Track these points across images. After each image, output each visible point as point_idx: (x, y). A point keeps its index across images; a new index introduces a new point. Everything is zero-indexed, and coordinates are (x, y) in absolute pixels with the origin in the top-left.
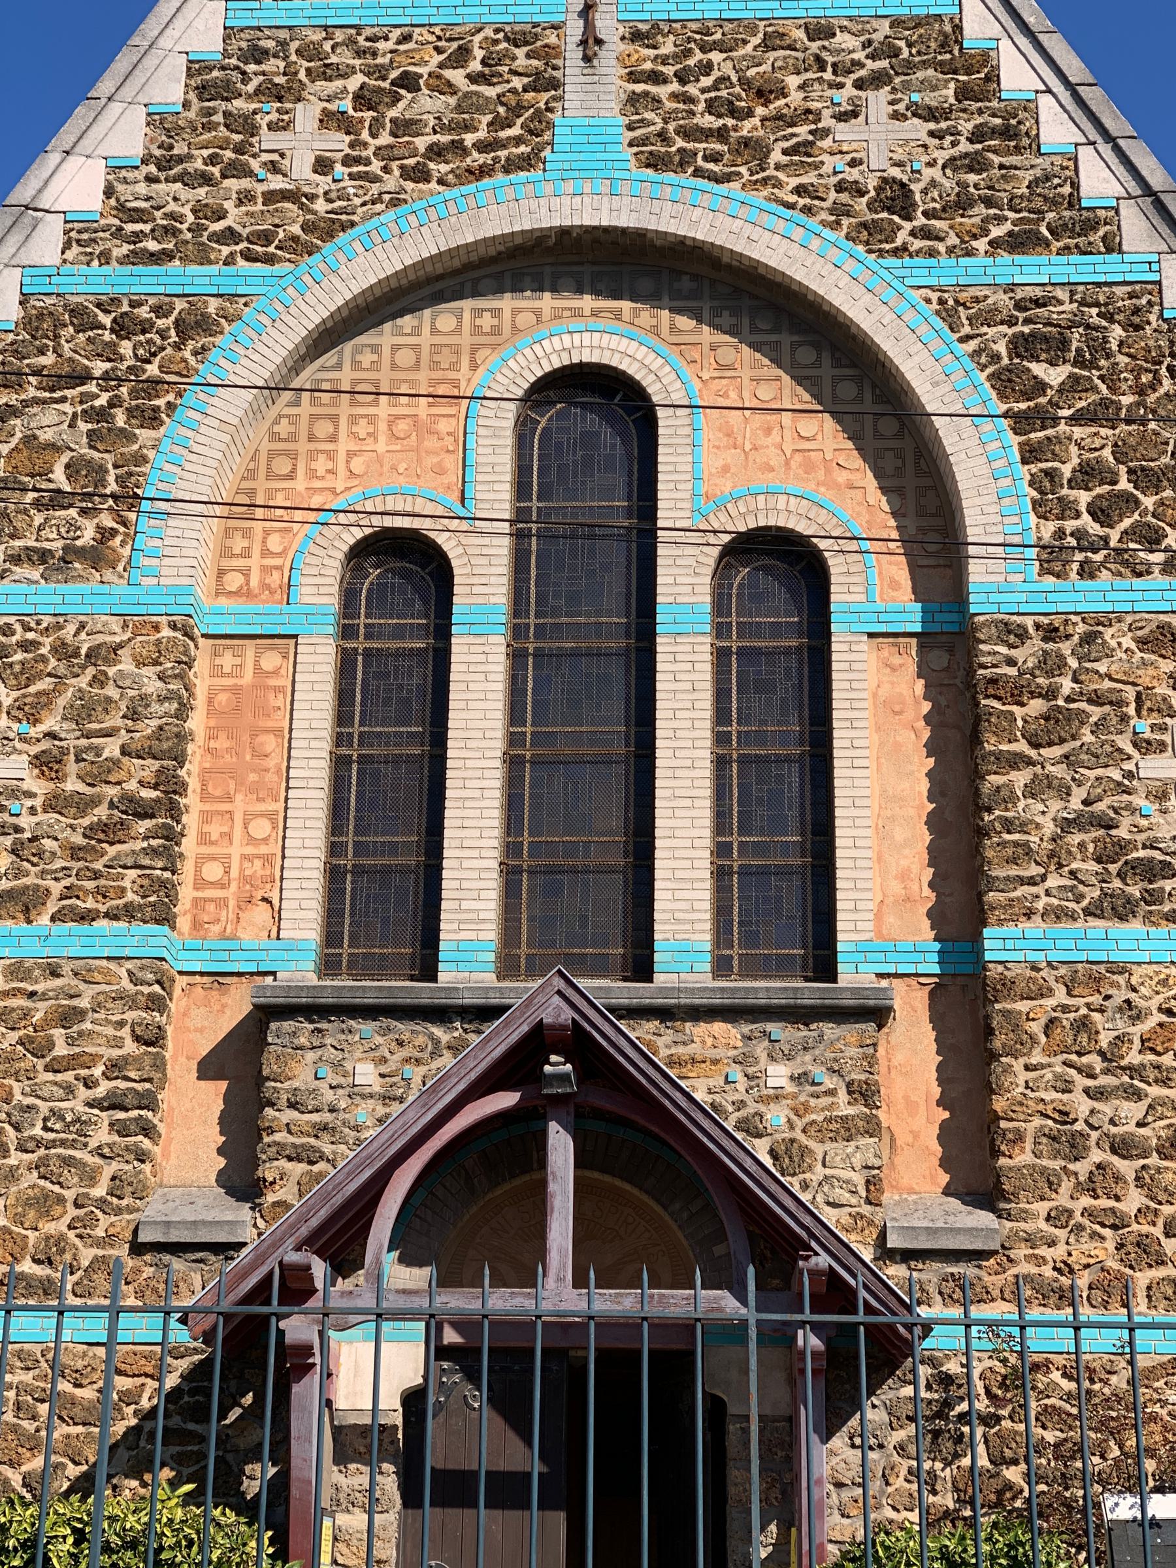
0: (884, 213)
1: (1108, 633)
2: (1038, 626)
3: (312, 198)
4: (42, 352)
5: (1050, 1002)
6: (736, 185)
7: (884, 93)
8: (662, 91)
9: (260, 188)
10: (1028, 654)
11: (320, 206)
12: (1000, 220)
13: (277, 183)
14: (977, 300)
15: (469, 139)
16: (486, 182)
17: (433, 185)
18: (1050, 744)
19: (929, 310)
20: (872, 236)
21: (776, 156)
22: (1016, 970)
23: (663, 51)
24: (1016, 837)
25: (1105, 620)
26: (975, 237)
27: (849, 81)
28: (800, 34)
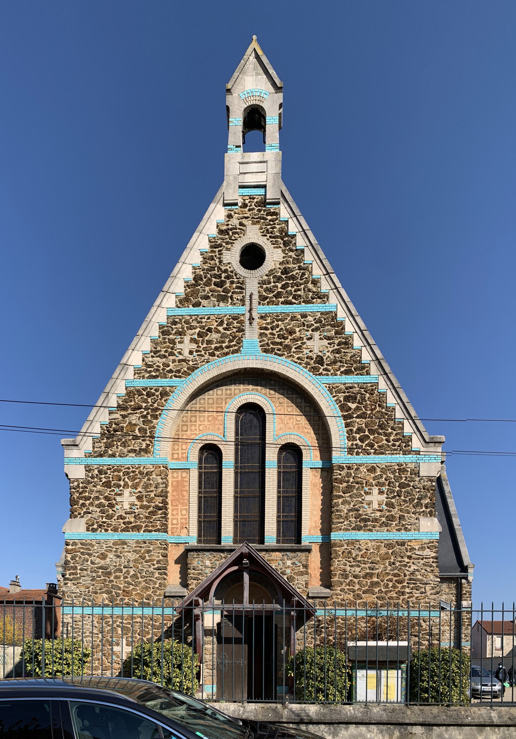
1: (361, 468)
25: (360, 465)
27: (310, 329)
28: (299, 317)
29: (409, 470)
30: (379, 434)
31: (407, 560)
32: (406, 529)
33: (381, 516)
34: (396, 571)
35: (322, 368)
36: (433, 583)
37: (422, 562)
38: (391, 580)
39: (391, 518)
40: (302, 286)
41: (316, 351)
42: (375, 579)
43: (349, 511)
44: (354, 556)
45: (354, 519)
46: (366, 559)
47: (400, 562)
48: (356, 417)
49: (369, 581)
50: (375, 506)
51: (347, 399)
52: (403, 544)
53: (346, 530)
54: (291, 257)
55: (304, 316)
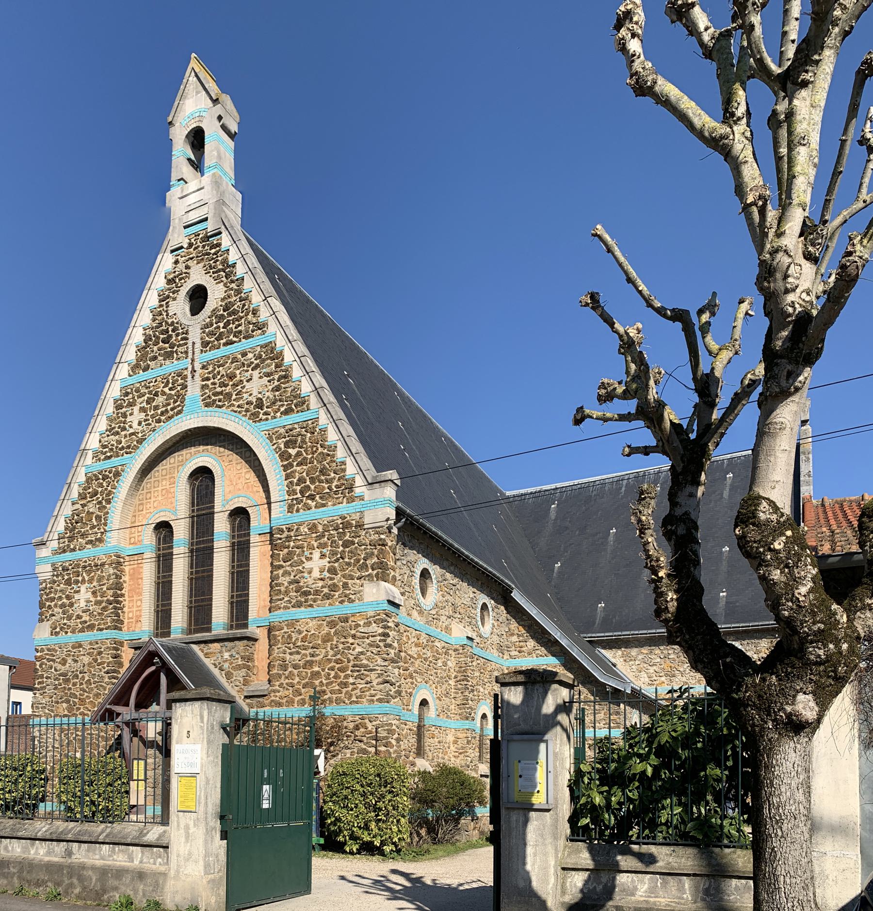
0: (256, 411)
1: (302, 527)
7: (258, 371)
8: (209, 383)
15: (169, 408)
20: (254, 417)
21: (234, 397)
25: (300, 524)
27: (250, 369)
28: (240, 356)
29: (354, 522)
30: (321, 481)
31: (351, 640)
32: (351, 601)
33: (322, 587)
34: (339, 656)
35: (262, 412)
36: (380, 668)
37: (368, 641)
38: (332, 669)
39: (333, 588)
40: (243, 320)
41: (255, 393)
42: (316, 669)
43: (290, 583)
44: (294, 639)
45: (295, 594)
46: (306, 644)
47: (343, 643)
48: (298, 465)
49: (309, 671)
50: (316, 574)
51: (287, 445)
52: (346, 620)
53: (286, 608)
54: (232, 289)
55: (244, 354)
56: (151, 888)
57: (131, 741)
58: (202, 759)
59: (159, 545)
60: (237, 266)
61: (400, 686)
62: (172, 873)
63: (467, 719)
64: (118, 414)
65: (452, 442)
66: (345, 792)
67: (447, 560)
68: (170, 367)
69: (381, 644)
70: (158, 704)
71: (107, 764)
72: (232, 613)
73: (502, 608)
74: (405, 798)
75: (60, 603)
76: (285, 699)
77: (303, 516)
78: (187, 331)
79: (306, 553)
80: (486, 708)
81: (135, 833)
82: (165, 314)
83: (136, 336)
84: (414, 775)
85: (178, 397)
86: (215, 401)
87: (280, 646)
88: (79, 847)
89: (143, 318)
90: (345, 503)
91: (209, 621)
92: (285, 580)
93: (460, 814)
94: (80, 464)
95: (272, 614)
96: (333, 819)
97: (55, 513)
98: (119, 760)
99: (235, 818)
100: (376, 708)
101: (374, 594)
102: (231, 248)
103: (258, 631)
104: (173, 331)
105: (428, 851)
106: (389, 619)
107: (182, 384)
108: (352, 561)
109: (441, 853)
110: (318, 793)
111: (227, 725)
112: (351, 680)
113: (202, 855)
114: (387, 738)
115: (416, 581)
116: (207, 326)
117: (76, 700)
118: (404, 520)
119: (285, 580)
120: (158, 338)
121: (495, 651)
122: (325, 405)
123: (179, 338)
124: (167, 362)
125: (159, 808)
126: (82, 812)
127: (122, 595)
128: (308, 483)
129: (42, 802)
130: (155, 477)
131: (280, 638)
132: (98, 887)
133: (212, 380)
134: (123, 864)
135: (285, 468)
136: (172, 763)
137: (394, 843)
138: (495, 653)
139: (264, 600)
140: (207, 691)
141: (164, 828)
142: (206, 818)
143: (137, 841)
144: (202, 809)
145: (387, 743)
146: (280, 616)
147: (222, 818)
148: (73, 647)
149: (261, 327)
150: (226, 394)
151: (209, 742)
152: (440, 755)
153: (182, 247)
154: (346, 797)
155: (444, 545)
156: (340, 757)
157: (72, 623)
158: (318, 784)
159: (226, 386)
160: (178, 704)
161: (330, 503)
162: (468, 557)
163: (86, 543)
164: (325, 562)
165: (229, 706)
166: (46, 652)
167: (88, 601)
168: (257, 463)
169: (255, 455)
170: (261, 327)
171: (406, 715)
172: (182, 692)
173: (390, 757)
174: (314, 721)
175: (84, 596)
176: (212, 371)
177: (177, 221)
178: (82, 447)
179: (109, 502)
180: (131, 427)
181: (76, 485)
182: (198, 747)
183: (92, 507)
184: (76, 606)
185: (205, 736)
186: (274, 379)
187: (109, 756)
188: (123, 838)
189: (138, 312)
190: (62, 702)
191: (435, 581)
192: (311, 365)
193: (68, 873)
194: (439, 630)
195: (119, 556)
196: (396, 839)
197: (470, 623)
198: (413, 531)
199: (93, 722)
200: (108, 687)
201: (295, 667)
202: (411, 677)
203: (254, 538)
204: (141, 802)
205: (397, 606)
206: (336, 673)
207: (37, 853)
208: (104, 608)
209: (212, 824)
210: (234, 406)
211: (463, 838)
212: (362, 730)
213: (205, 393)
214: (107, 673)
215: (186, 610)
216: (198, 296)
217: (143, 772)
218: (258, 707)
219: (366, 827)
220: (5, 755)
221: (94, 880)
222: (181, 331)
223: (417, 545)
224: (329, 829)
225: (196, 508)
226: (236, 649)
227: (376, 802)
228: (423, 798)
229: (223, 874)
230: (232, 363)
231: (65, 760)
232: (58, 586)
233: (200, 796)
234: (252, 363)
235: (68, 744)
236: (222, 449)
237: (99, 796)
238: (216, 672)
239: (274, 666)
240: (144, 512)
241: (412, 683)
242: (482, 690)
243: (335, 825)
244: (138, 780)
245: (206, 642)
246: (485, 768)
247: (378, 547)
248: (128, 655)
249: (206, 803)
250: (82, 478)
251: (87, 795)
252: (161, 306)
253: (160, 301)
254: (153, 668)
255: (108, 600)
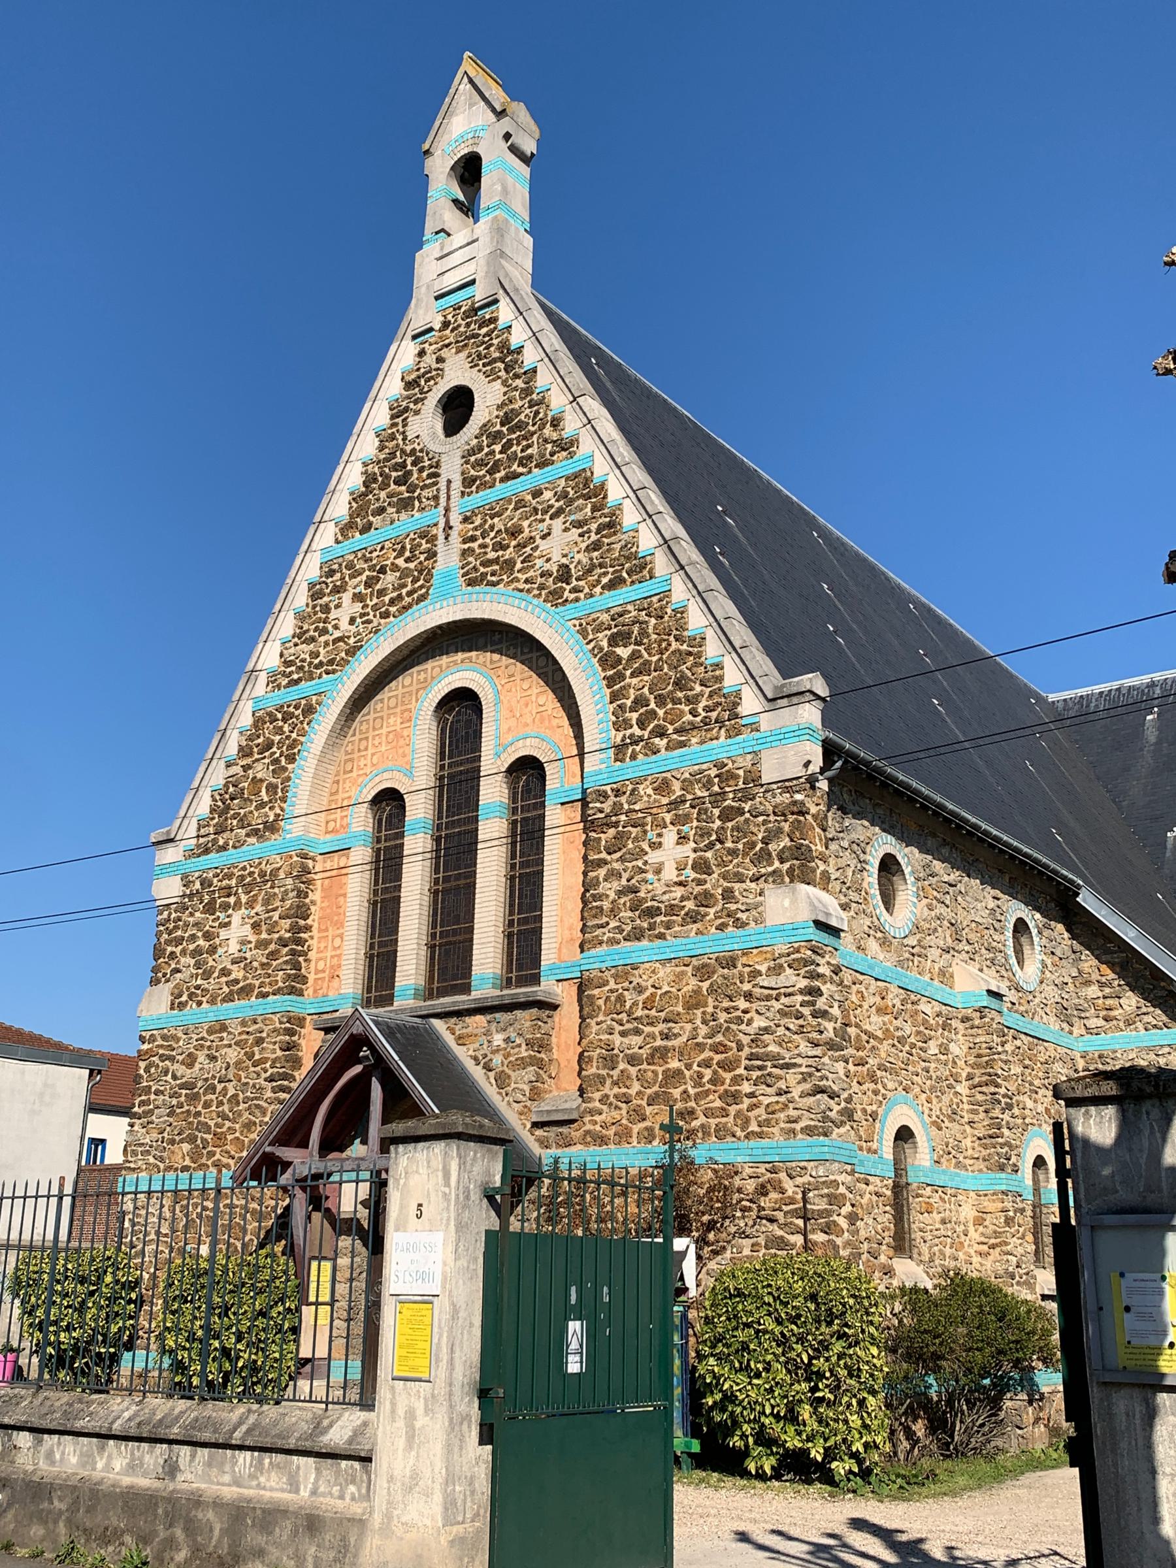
0: (558, 586)
1: (641, 787)
2: (613, 790)
3: (349, 637)
4: (258, 737)
5: (607, 988)
6: (501, 586)
8: (475, 545)
9: (331, 638)
10: (607, 807)
11: (352, 641)
12: (605, 574)
13: (337, 634)
14: (594, 620)
15: (404, 591)
16: (410, 611)
17: (392, 618)
18: (615, 852)
19: (573, 630)
20: (555, 597)
21: (519, 566)
22: (594, 973)
23: (477, 523)
24: (598, 903)
25: (638, 782)
26: (594, 586)
27: (547, 517)
28: (529, 497)
29: (741, 772)
30: (677, 701)
31: (742, 1004)
32: (740, 924)
33: (683, 899)
34: (719, 1038)
35: (568, 588)
36: (804, 1062)
37: (777, 1005)
38: (707, 1064)
39: (705, 899)
40: (535, 438)
41: (556, 556)
42: (674, 1064)
43: (620, 893)
44: (628, 1005)
45: (630, 914)
46: (653, 1012)
47: (727, 1010)
48: (632, 675)
49: (660, 1070)
51: (613, 641)
52: (731, 963)
53: (613, 942)
54: (516, 389)
55: (537, 493)
56: (332, 1555)
57: (309, 1218)
58: (445, 1264)
59: (379, 831)
60: (525, 351)
61: (849, 1100)
62: (377, 1519)
63: (1002, 1168)
64: (314, 607)
65: (930, 610)
66: (742, 1335)
67: (934, 835)
68: (408, 523)
69: (806, 1011)
70: (364, 1142)
71: (258, 1268)
72: (510, 954)
73: (1060, 927)
74: (875, 1351)
75: (192, 947)
76: (613, 1129)
77: (642, 766)
78: (438, 462)
79: (649, 835)
80: (1042, 1145)
81: (304, 1426)
82: (400, 438)
83: (350, 477)
84: (893, 1297)
85: (420, 572)
86: (484, 575)
87: (601, 1018)
88: (193, 1456)
89: (364, 446)
90: (722, 739)
91: (468, 973)
92: (609, 889)
93: (1002, 1387)
94: (245, 696)
95: (586, 954)
96: (718, 1397)
97: (195, 784)
98: (282, 1260)
99: (511, 1396)
100: (802, 1148)
101: (787, 908)
102: (514, 324)
103: (558, 989)
104: (414, 464)
105: (932, 1476)
106: (818, 959)
107: (429, 551)
108: (740, 846)
109: (962, 1481)
110: (684, 1336)
111: (497, 1191)
112: (746, 1088)
113: (440, 1480)
114: (828, 1213)
115: (871, 879)
116: (471, 452)
117: (209, 1137)
118: (839, 764)
119: (609, 889)
120: (388, 477)
121: (1053, 1019)
122: (682, 568)
123: (425, 474)
124: (403, 516)
125: (356, 1365)
126: (203, 1374)
127: (308, 928)
128: (653, 705)
129: (128, 1350)
130: (375, 711)
131: (601, 1002)
132: (224, 1550)
133: (480, 541)
134: (277, 1495)
135: (610, 681)
136: (386, 1272)
137: (855, 1456)
138: (1054, 1025)
139: (570, 929)
140: (459, 1120)
141: (363, 1415)
142: (450, 1394)
143: (308, 1445)
144: (441, 1374)
145: (828, 1225)
146: (601, 958)
147: (483, 1394)
148: (210, 1031)
149: (567, 446)
150: (505, 561)
151: (460, 1227)
152: (948, 1251)
153: (431, 330)
154: (745, 1347)
155: (924, 808)
156: (728, 1254)
157: (211, 985)
158: (684, 1316)
159: (504, 548)
160: (401, 1148)
161: (694, 740)
162: (976, 827)
163: (248, 835)
164: (687, 850)
165: (499, 1150)
166: (160, 1042)
167: (244, 942)
168: (558, 677)
169: (555, 662)
170: (567, 446)
171: (867, 1163)
172: (410, 1123)
173: (837, 1256)
174: (672, 1179)
175: (236, 932)
176: (481, 525)
177: (423, 290)
178: (250, 667)
179: (291, 759)
180: (336, 627)
181: (236, 732)
182: (439, 1237)
183: (261, 771)
184: (220, 951)
185: (452, 1215)
186: (589, 531)
187: (263, 1252)
188: (279, 1436)
189: (354, 438)
190: (182, 1141)
191: (910, 879)
192: (656, 501)
193: (166, 1514)
194: (927, 978)
195: (304, 856)
196: (858, 1446)
197: (992, 961)
198: (858, 783)
199: (239, 1180)
200: (272, 1108)
201: (633, 1060)
202: (873, 1079)
203: (554, 815)
204: (322, 1352)
205: (835, 932)
206: (715, 1072)
207: (108, 1467)
208: (272, 953)
209: (462, 1408)
210: (518, 580)
211: (1011, 1442)
212: (774, 1195)
213: (468, 563)
214: (271, 1079)
215: (424, 951)
216: (458, 406)
217: (328, 1285)
218: (558, 1146)
219: (792, 1417)
220: (67, 1249)
221: (217, 1532)
222: (427, 463)
223: (870, 808)
224: (710, 1420)
225: (447, 762)
226: (517, 1026)
227: (811, 1358)
228: (915, 1348)
229: (483, 1523)
230: (516, 509)
231: (179, 1261)
232: (192, 915)
233: (439, 1343)
234: (552, 506)
235: (186, 1226)
236: (496, 656)
237: (239, 1340)
238: (477, 1073)
239: (590, 1059)
240: (354, 774)
241: (876, 1092)
242: (1030, 1104)
243: (723, 1410)
244: (317, 1304)
245: (459, 1014)
246: (1047, 1280)
247: (791, 818)
248: (311, 1042)
249: (451, 1361)
250: (245, 719)
251: (217, 1337)
252: (394, 425)
253: (393, 417)
254: (357, 1069)
255: (280, 939)
